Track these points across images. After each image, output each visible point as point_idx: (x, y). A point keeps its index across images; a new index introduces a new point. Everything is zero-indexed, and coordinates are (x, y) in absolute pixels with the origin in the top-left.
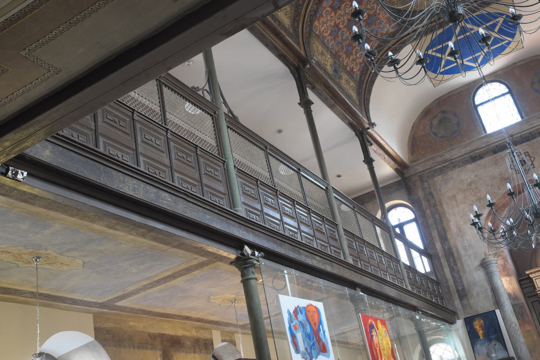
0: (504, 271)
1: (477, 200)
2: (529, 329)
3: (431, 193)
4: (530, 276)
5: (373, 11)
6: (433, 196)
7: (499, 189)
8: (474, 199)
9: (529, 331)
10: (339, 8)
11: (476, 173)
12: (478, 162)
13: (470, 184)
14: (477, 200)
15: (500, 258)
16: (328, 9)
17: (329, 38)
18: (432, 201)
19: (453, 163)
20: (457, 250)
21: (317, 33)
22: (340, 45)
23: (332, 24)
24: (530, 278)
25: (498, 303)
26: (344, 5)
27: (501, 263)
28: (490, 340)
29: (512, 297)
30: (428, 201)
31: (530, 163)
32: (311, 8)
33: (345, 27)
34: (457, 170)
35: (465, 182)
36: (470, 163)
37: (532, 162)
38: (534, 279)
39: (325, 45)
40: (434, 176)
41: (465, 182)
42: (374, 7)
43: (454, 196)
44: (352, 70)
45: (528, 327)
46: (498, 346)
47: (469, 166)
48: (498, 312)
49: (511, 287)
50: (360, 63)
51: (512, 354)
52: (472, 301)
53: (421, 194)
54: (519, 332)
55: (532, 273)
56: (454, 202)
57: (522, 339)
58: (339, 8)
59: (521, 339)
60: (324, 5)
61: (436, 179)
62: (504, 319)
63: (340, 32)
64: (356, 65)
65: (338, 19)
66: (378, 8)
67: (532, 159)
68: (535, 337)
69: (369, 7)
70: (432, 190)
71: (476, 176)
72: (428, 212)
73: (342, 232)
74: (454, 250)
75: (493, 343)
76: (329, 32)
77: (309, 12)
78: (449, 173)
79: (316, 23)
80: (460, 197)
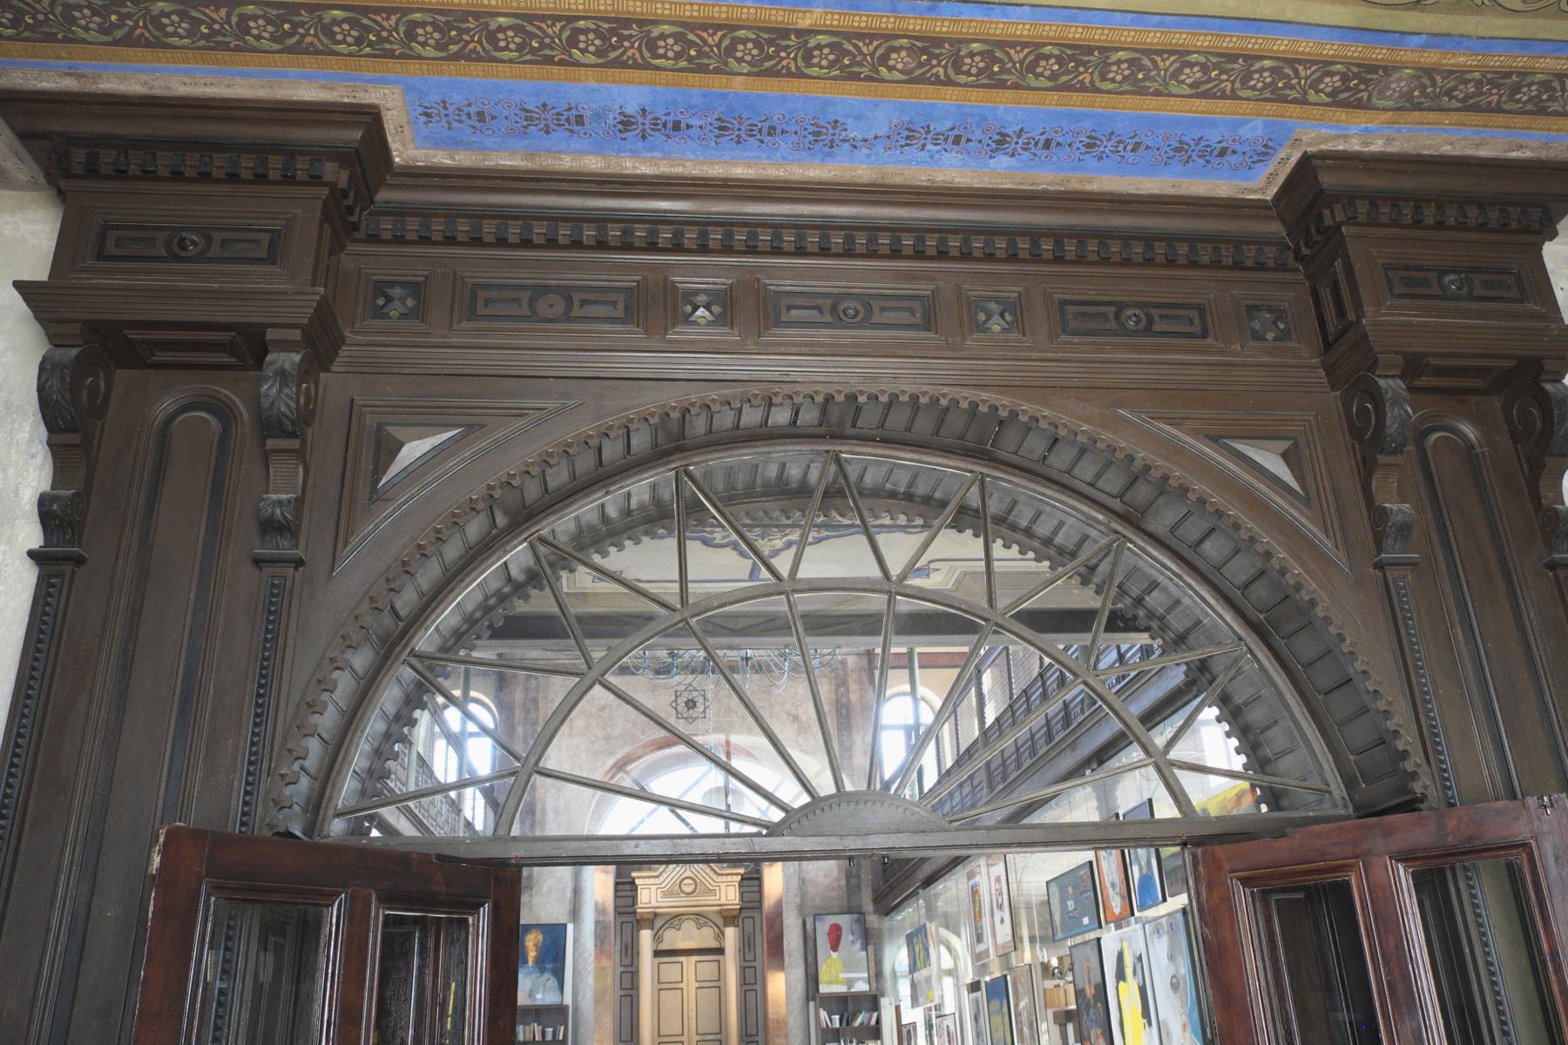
3: (535, 701)
4: (637, 882)
6: (537, 708)
7: (643, 732)
8: (600, 733)
9: (604, 968)
13: (602, 709)
18: (533, 715)
20: (543, 809)
24: (633, 883)
25: (575, 914)
28: (542, 971)
29: (600, 910)
30: (527, 712)
31: (701, 709)
45: (605, 963)
46: (553, 982)
48: (570, 927)
51: (568, 1000)
52: (535, 900)
53: (519, 696)
54: (591, 967)
57: (590, 980)
59: (589, 980)
62: (575, 941)
68: (609, 980)
70: (540, 696)
72: (520, 730)
73: (414, 755)
74: (539, 807)
75: (547, 975)
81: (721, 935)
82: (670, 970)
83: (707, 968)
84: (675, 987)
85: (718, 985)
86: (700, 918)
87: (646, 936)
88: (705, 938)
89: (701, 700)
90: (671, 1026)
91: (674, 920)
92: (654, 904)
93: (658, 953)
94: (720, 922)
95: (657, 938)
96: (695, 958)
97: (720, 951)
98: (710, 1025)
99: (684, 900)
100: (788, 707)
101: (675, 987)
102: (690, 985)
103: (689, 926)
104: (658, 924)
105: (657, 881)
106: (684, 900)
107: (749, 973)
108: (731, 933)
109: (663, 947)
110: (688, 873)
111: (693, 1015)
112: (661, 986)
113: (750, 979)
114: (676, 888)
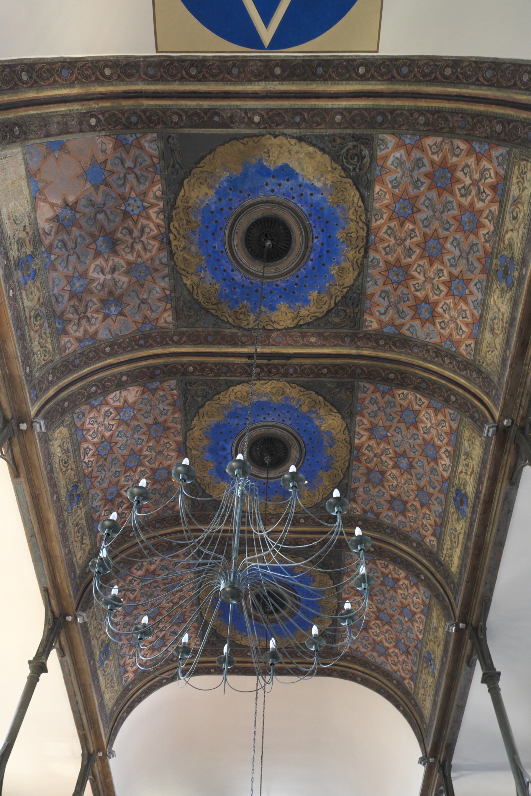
5: (392, 225)
10: (426, 300)
16: (439, 327)
17: (470, 299)
21: (472, 342)
22: (470, 256)
23: (450, 301)
26: (418, 294)
32: (450, 370)
33: (442, 262)
39: (481, 317)
42: (386, 232)
44: (494, 188)
50: (478, 161)
58: (426, 300)
60: (437, 340)
63: (456, 271)
64: (482, 176)
65: (441, 291)
66: (381, 221)
69: (392, 241)
76: (464, 307)
77: (455, 372)
79: (462, 349)
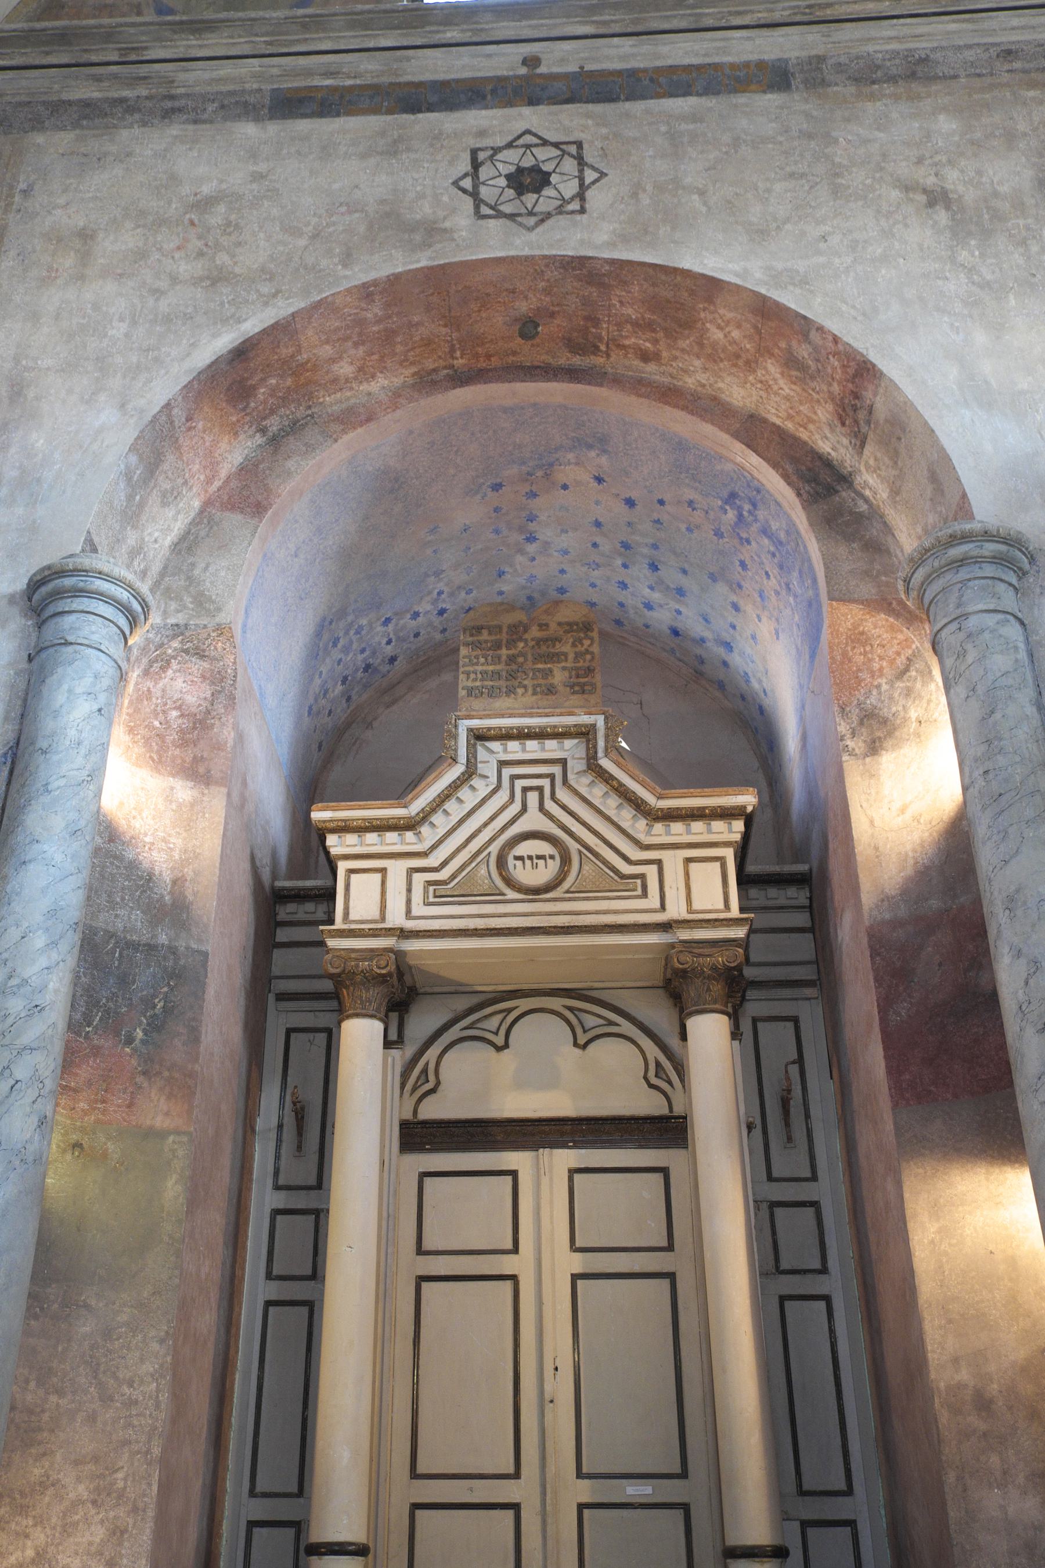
0: (184, 743)
1: (196, 281)
2: (159, 1122)
8: (185, 268)
11: (262, 167)
12: (303, 125)
13: (205, 204)
14: (196, 281)
15: (198, 666)
19: (172, 97)
27: (191, 699)
34: (175, 130)
35: (186, 190)
36: (257, 119)
37: (583, 187)
38: (342, 867)
40: (37, 124)
41: (186, 190)
43: (86, 236)
47: (249, 130)
49: (177, 842)
55: (344, 828)
56: (69, 261)
61: (40, 139)
67: (590, 176)
68: (173, 1190)
71: (258, 177)
78: (125, 133)
80: (112, 245)
81: (671, 1066)
82: (467, 1207)
83: (622, 1201)
84: (485, 1271)
85: (670, 1266)
86: (583, 1005)
87: (361, 1037)
88: (608, 1078)
89: (569, 165)
90: (467, 1433)
91: (486, 1009)
92: (396, 917)
93: (416, 1135)
94: (658, 1014)
95: (416, 1078)
96: (565, 1158)
97: (670, 1130)
98: (633, 1435)
99: (516, 911)
100: (904, 169)
101: (485, 1271)
102: (549, 1261)
103: (541, 1036)
104: (422, 1022)
105: (409, 841)
106: (516, 911)
107: (795, 1226)
108: (709, 1035)
109: (432, 1110)
110: (533, 821)
111: (562, 1389)
112: (424, 1272)
113: (798, 1249)
114: (486, 873)
